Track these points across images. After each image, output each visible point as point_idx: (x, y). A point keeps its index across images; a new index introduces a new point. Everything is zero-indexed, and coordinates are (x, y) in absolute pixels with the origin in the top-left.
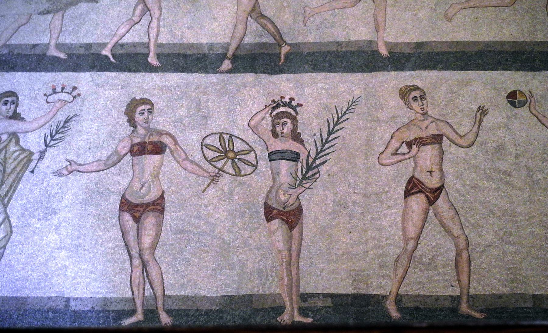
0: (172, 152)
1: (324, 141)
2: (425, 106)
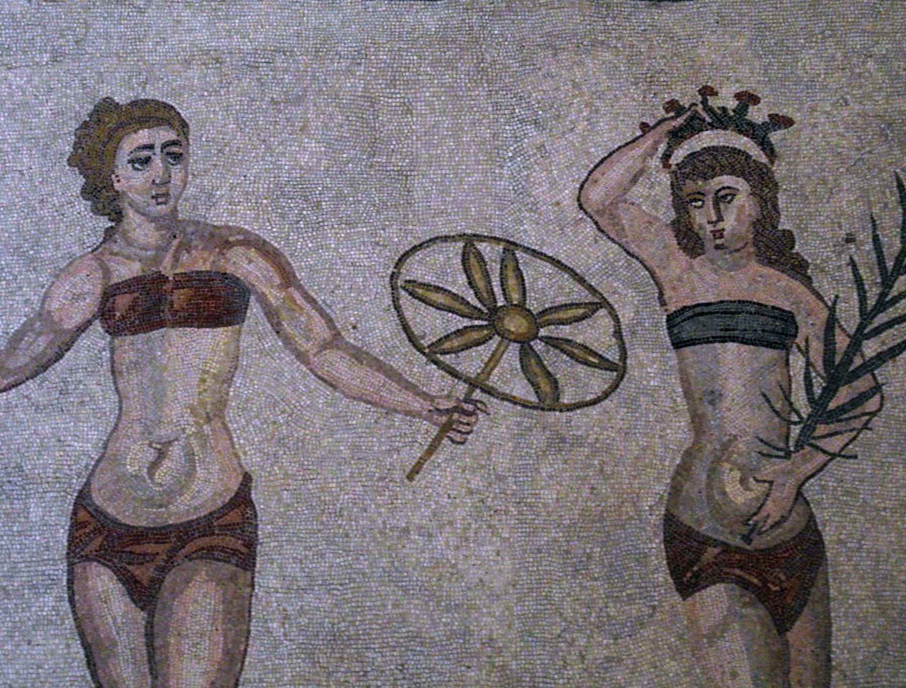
0: (271, 314)
1: (890, 264)
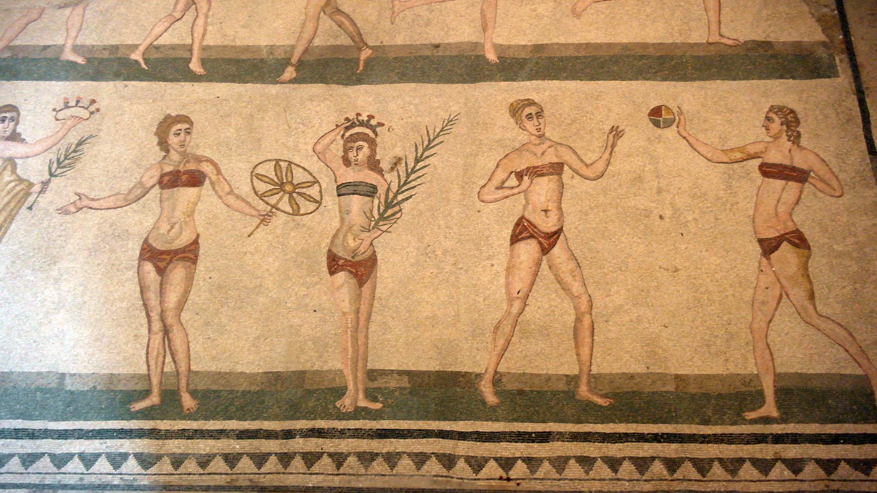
0: (212, 184)
1: (409, 171)
2: (541, 126)
